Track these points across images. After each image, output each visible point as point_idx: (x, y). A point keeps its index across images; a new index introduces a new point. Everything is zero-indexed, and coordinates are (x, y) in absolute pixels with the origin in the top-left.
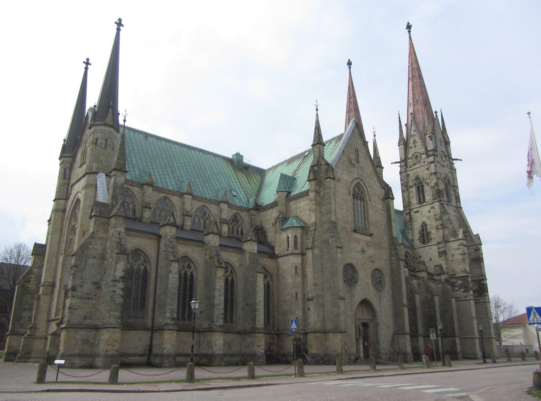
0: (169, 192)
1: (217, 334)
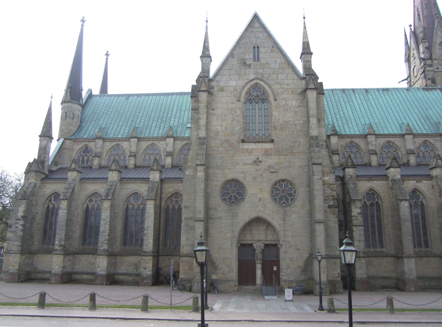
1: (100, 257)
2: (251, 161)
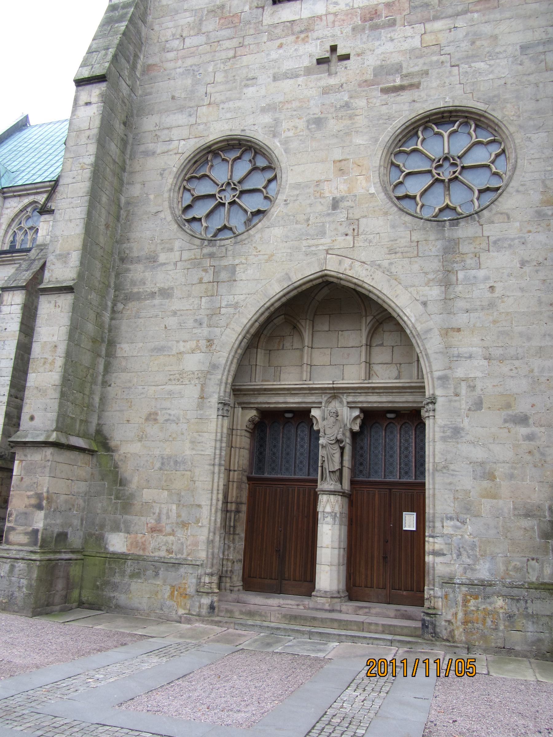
0: (37, 188)
2: (306, 62)
